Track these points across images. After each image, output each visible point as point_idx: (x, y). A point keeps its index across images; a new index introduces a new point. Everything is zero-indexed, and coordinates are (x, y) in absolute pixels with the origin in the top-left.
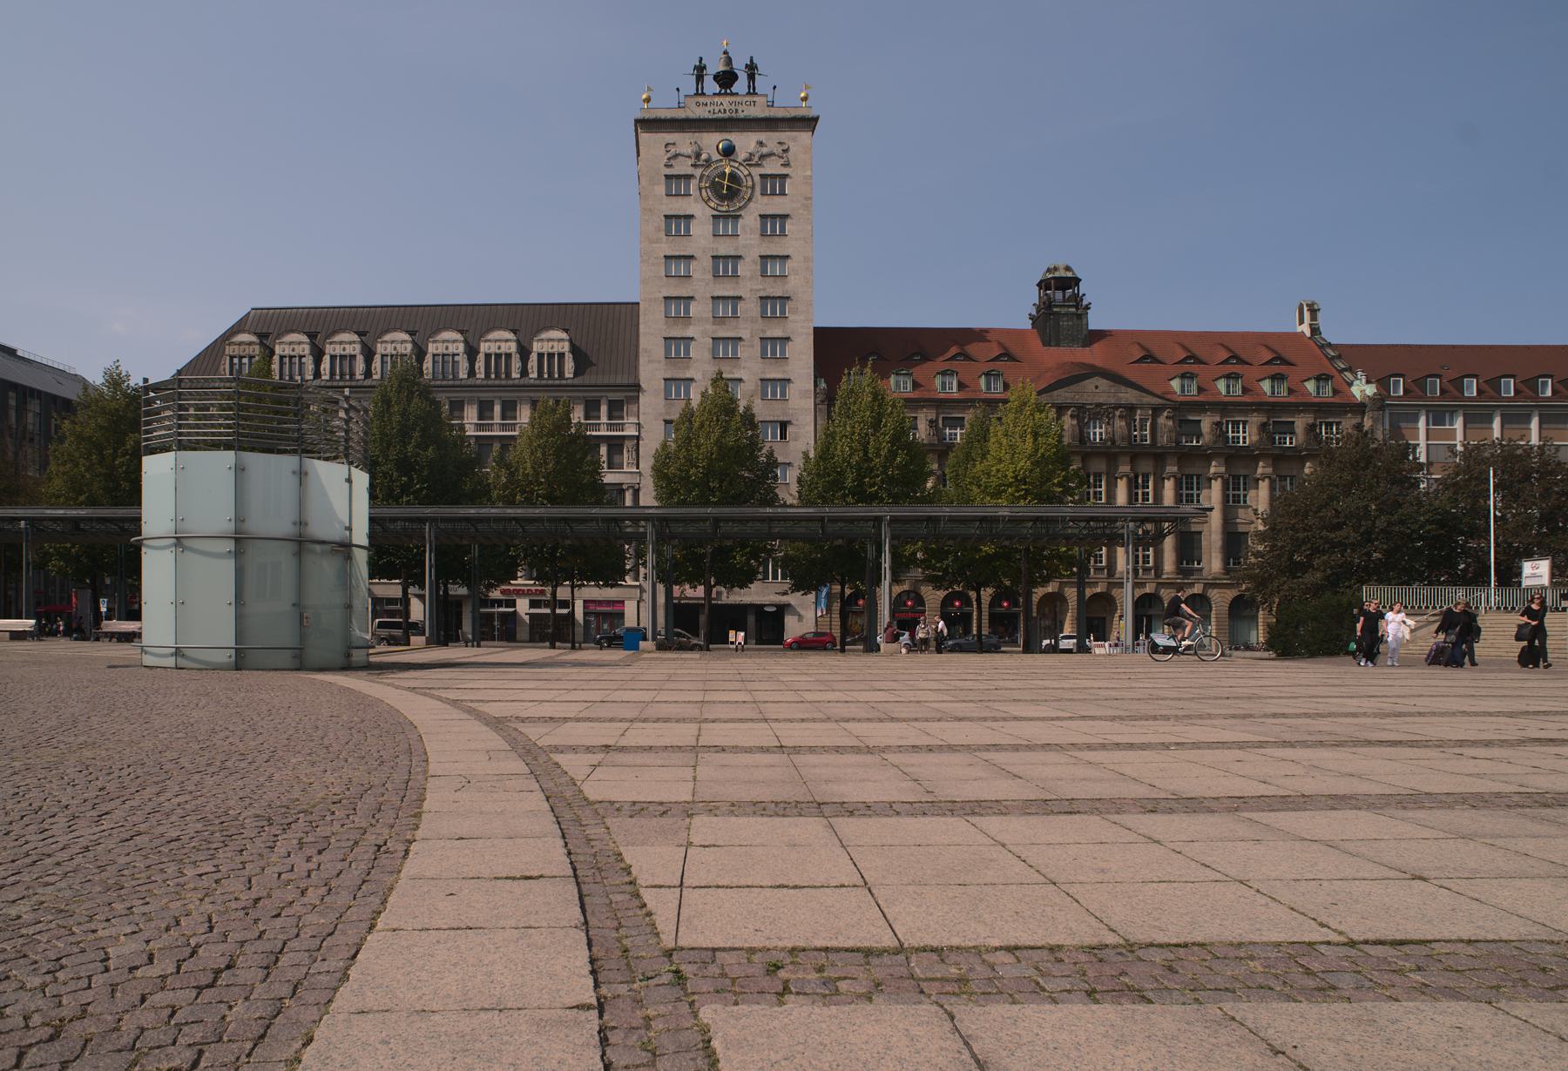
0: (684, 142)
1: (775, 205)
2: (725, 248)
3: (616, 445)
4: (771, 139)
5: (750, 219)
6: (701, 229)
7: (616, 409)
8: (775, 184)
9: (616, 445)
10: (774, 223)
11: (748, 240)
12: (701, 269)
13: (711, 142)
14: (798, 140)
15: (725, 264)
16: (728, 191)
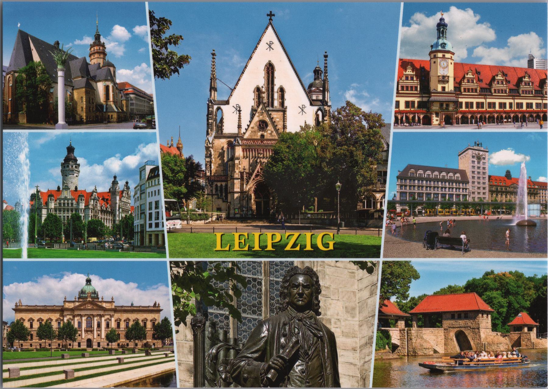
0: (474, 152)
1: (484, 161)
2: (479, 165)
3: (466, 189)
4: (484, 153)
5: (481, 163)
6: (476, 163)
7: (466, 184)
8: (484, 158)
9: (466, 189)
10: (484, 163)
11: (481, 165)
12: (476, 168)
13: (477, 152)
14: (487, 154)
15: (479, 168)
16: (479, 158)
